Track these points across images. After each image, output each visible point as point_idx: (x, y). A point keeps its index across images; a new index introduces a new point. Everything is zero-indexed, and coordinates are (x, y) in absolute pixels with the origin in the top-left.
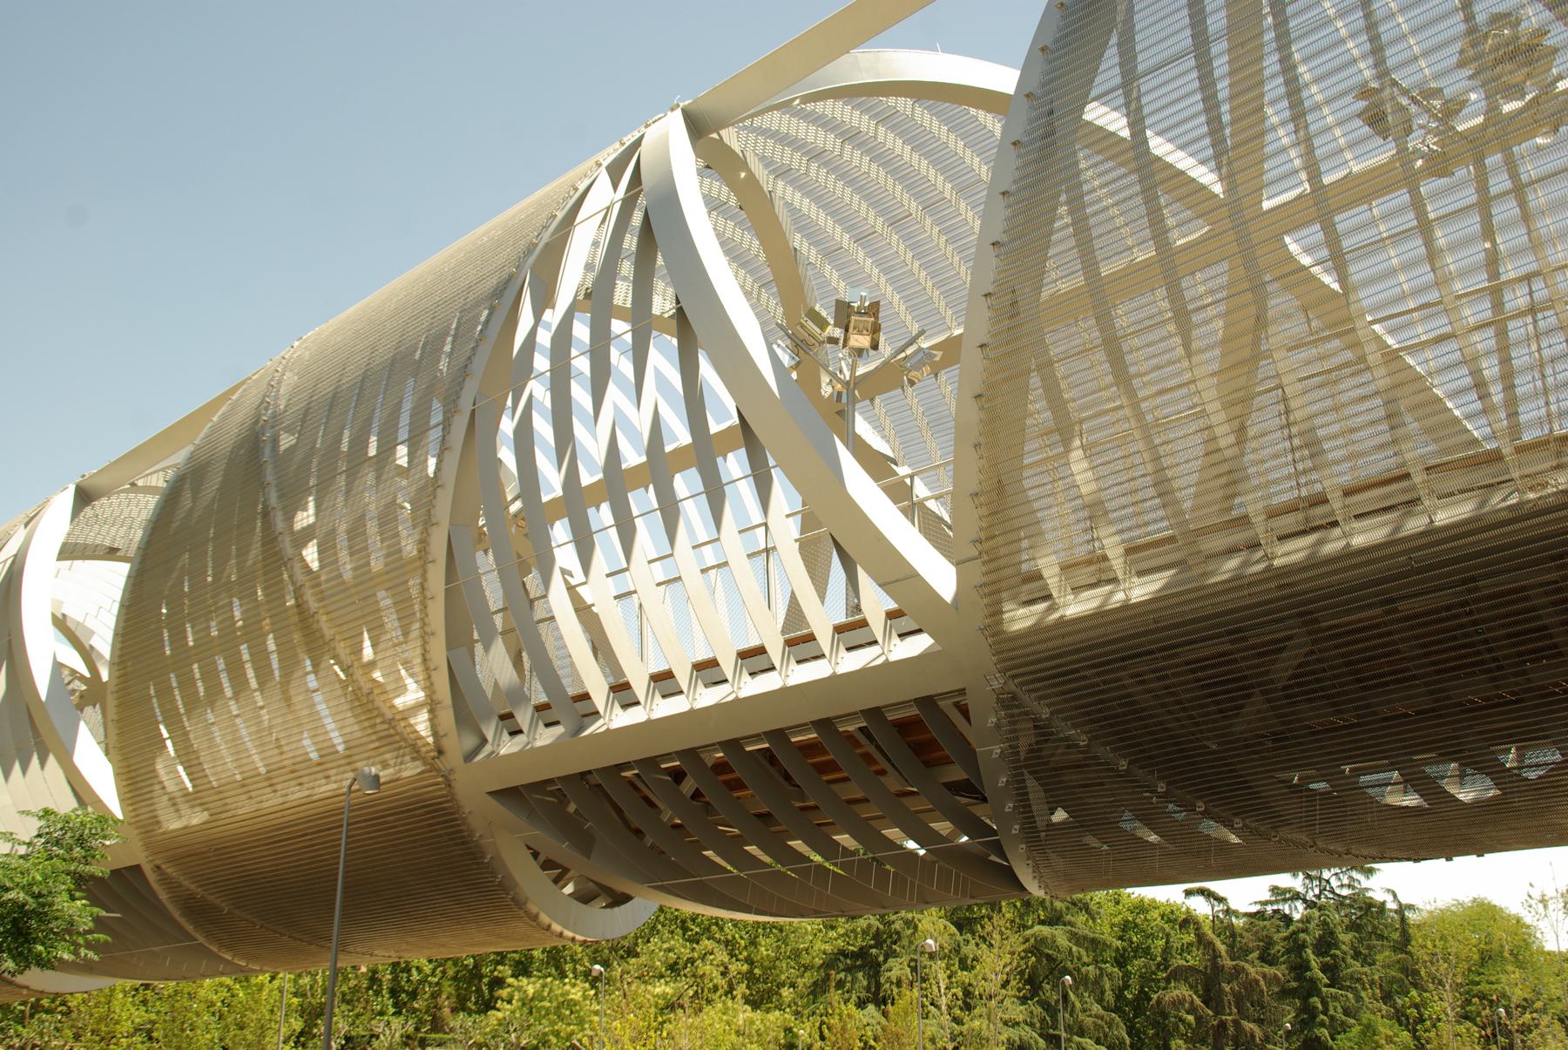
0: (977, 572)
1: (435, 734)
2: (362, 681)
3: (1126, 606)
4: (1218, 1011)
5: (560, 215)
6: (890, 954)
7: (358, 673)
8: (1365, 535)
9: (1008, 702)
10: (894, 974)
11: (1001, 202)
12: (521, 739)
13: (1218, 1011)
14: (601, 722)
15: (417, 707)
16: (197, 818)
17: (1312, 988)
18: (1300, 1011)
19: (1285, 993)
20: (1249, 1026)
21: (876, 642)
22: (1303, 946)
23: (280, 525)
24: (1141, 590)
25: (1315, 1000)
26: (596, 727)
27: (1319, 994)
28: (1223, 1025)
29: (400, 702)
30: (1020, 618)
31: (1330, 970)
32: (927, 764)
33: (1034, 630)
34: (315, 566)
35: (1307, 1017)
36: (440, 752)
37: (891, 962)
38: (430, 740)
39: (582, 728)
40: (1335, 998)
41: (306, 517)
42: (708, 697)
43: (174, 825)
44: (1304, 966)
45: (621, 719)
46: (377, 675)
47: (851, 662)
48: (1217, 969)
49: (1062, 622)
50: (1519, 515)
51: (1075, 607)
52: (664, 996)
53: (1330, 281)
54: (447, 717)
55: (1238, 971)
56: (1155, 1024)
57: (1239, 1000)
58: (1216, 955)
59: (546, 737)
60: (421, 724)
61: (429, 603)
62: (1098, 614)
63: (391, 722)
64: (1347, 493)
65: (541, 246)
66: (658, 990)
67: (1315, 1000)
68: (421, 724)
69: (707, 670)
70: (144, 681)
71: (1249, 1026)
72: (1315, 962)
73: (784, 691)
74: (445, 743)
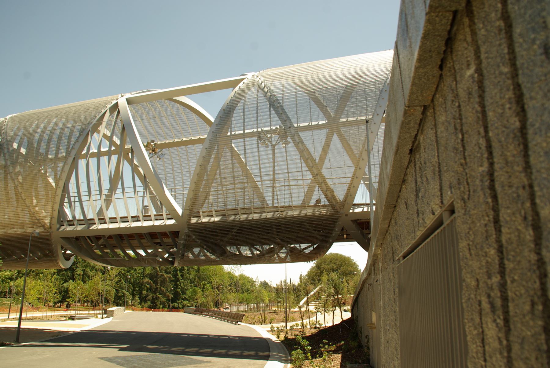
0: (188, 212)
1: (50, 223)
2: (32, 210)
3: (214, 222)
4: (156, 285)
5: (98, 117)
6: (77, 267)
8: (256, 216)
9: (187, 234)
10: (78, 272)
11: (205, 150)
13: (156, 285)
14: (95, 226)
17: (178, 280)
18: (174, 285)
19: (171, 281)
20: (162, 288)
21: (163, 219)
22: (177, 270)
23: (11, 169)
24: (217, 219)
25: (178, 283)
26: (94, 227)
27: (179, 281)
28: (157, 288)
29: (42, 215)
30: (194, 220)
31: (182, 276)
32: (152, 238)
33: (196, 223)
34: (21, 181)
35: (176, 286)
36: (51, 228)
37: (77, 269)
38: (48, 225)
39: (89, 227)
40: (183, 282)
41: (18, 169)
42: (123, 225)
44: (177, 275)
45: (101, 227)
46: (37, 209)
47: (158, 223)
48: (157, 275)
49: (202, 223)
50: (279, 218)
51: (205, 220)
52: (8, 275)
53: (243, 160)
54: (55, 221)
55: (162, 275)
56: (139, 287)
57: (162, 282)
58: (157, 271)
59: (80, 228)
60: (47, 221)
61: (56, 197)
62: (208, 223)
63: (38, 220)
64: (254, 208)
65: (93, 123)
66: (6, 274)
67: (178, 283)
68: (47, 221)
69: (124, 219)
71: (162, 288)
72: (179, 274)
73: (142, 227)
74: (52, 226)
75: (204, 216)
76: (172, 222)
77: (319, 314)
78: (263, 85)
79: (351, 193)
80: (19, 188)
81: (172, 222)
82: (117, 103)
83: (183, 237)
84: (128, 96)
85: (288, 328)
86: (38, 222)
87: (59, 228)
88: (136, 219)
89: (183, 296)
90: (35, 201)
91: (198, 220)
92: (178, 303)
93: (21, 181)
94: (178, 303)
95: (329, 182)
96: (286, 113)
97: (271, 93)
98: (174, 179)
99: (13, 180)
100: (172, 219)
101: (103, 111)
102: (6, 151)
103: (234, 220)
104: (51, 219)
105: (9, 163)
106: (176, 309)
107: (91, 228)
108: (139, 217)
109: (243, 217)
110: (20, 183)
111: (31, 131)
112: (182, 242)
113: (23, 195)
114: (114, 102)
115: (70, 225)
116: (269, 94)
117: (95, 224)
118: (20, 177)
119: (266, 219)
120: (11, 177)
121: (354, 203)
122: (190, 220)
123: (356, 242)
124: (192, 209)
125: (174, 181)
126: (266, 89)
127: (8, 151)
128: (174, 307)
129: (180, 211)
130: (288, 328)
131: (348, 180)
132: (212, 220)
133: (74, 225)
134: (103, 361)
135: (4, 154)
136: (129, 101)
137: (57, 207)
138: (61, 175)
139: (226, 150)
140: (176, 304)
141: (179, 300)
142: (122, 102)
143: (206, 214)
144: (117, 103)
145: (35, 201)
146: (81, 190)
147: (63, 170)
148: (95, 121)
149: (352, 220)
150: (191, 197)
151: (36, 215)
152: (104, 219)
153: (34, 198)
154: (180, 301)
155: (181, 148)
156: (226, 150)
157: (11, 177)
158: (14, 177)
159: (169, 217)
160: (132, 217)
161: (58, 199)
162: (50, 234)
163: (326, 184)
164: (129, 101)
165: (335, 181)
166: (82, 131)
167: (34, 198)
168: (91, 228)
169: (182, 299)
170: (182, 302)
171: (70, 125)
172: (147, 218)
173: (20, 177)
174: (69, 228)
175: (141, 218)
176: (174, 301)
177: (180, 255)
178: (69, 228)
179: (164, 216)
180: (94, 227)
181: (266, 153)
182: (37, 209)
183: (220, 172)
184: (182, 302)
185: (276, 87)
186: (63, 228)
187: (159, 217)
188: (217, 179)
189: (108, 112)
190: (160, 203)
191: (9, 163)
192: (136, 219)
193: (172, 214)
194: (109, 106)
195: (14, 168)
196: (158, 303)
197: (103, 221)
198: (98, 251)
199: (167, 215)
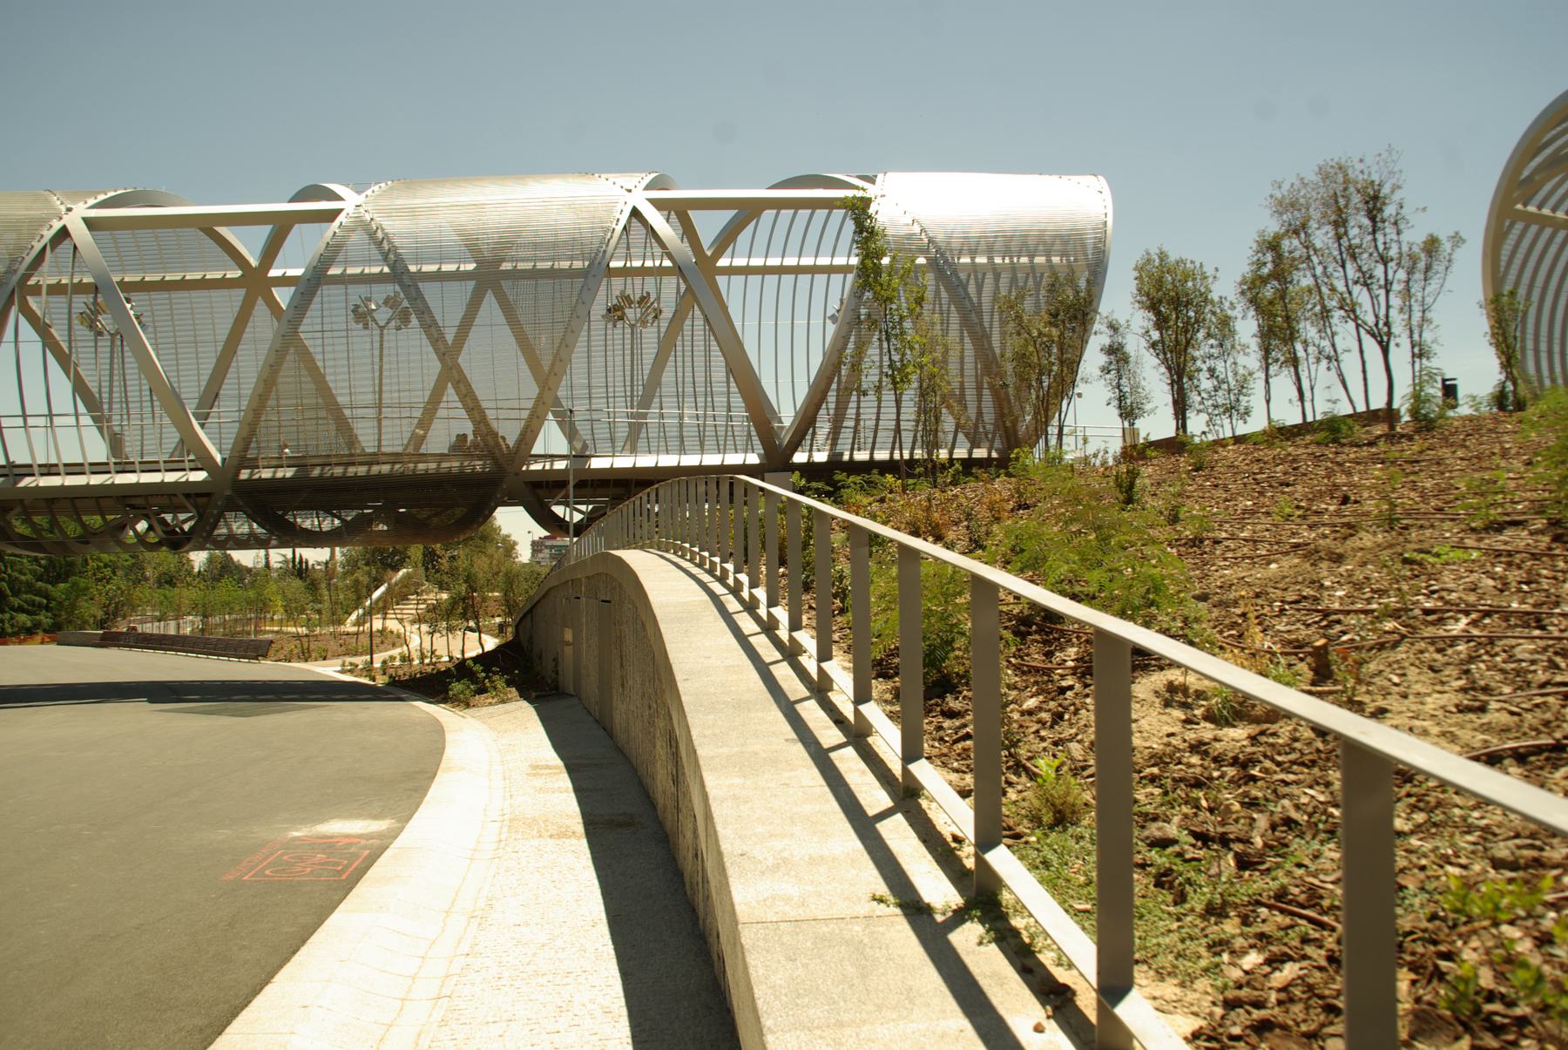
5: (28, 260)
24: (289, 473)
30: (244, 475)
42: (96, 480)
50: (402, 475)
51: (266, 474)
62: (273, 479)
76: (200, 476)
77: (437, 635)
78: (380, 235)
79: (529, 433)
81: (200, 476)
82: (64, 233)
85: (377, 665)
89: (16, 602)
95: (490, 415)
96: (424, 299)
97: (390, 242)
101: (38, 247)
103: (321, 477)
107: (22, 484)
109: (338, 471)
114: (57, 225)
116: (392, 256)
119: (380, 475)
121: (534, 452)
122: (238, 474)
123: (521, 508)
126: (386, 245)
129: (218, 458)
130: (377, 665)
131: (525, 414)
132: (280, 474)
139: (260, 301)
144: (64, 233)
149: (526, 483)
150: (245, 434)
154: (7, 616)
156: (260, 301)
163: (487, 425)
165: (503, 414)
168: (22, 484)
169: (13, 609)
170: (12, 618)
181: (363, 340)
184: (12, 618)
185: (395, 226)
194: (48, 234)
198: (21, 528)
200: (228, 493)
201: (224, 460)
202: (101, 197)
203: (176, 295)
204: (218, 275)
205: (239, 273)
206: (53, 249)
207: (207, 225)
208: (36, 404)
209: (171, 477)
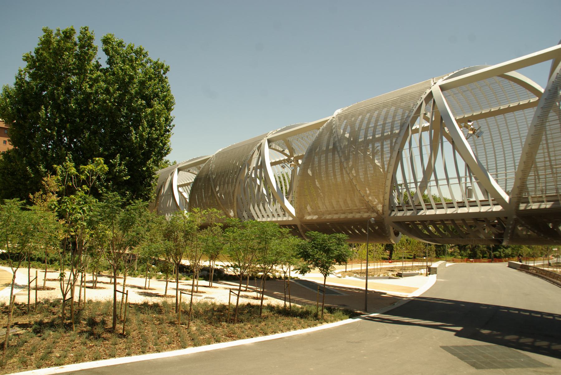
1: (383, 210)
2: (366, 199)
3: (545, 209)
5: (415, 110)
7: (365, 198)
12: (403, 212)
15: (377, 204)
16: (315, 217)
23: (345, 164)
24: (548, 205)
26: (421, 213)
29: (375, 203)
30: (522, 207)
33: (525, 210)
34: (355, 175)
38: (381, 211)
39: (418, 213)
43: (308, 218)
45: (429, 212)
46: (370, 198)
49: (531, 209)
51: (535, 206)
54: (387, 208)
59: (409, 213)
61: (386, 188)
62: (539, 210)
63: (372, 208)
68: (380, 208)
70: (301, 188)
73: (468, 213)
74: (385, 213)
75: (534, 202)
80: (354, 181)
81: (498, 208)
82: (431, 93)
83: (511, 222)
84: (441, 82)
86: (373, 209)
87: (391, 213)
88: (461, 205)
90: (368, 192)
91: (526, 207)
92: (500, 252)
93: (355, 175)
94: (500, 252)
98: (494, 148)
99: (348, 174)
100: (497, 204)
101: (419, 103)
102: (339, 149)
104: (383, 206)
105: (343, 160)
106: (498, 259)
107: (419, 214)
108: (464, 202)
110: (354, 177)
111: (357, 129)
112: (510, 227)
113: (357, 187)
114: (428, 91)
115: (399, 210)
117: (422, 209)
118: (353, 172)
120: (346, 171)
122: (518, 206)
124: (520, 193)
125: (494, 150)
127: (341, 149)
128: (495, 256)
129: (507, 198)
132: (543, 206)
133: (403, 210)
134: (446, 352)
135: (338, 152)
136: (442, 88)
137: (387, 196)
138: (388, 168)
140: (497, 253)
141: (500, 248)
142: (436, 90)
143: (536, 200)
144: (431, 93)
145: (368, 192)
146: (407, 178)
147: (389, 163)
148: (412, 114)
151: (370, 203)
152: (430, 205)
153: (367, 189)
154: (502, 250)
155: (500, 117)
157: (346, 171)
158: (348, 172)
159: (495, 202)
160: (458, 203)
161: (388, 189)
162: (383, 219)
164: (442, 88)
166: (402, 126)
167: (367, 189)
168: (419, 214)
169: (504, 247)
170: (504, 251)
171: (391, 121)
172: (473, 204)
173: (353, 172)
174: (400, 214)
175: (467, 204)
176: (495, 249)
177: (509, 235)
178: (400, 214)
179: (491, 202)
180: (421, 213)
182: (370, 198)
183: (546, 137)
184: (504, 251)
186: (393, 214)
187: (484, 203)
188: (543, 144)
189: (424, 103)
190: (487, 190)
191: (343, 160)
192: (461, 205)
193: (498, 200)
194: (424, 96)
195: (348, 164)
196: (478, 252)
197: (429, 207)
199: (492, 200)
200: (515, 217)
201: (510, 200)
202: (450, 75)
203: (508, 115)
204: (526, 102)
205: (537, 98)
206: (427, 103)
207: (501, 73)
208: (452, 173)
209: (484, 209)
